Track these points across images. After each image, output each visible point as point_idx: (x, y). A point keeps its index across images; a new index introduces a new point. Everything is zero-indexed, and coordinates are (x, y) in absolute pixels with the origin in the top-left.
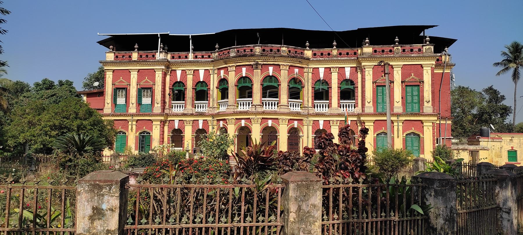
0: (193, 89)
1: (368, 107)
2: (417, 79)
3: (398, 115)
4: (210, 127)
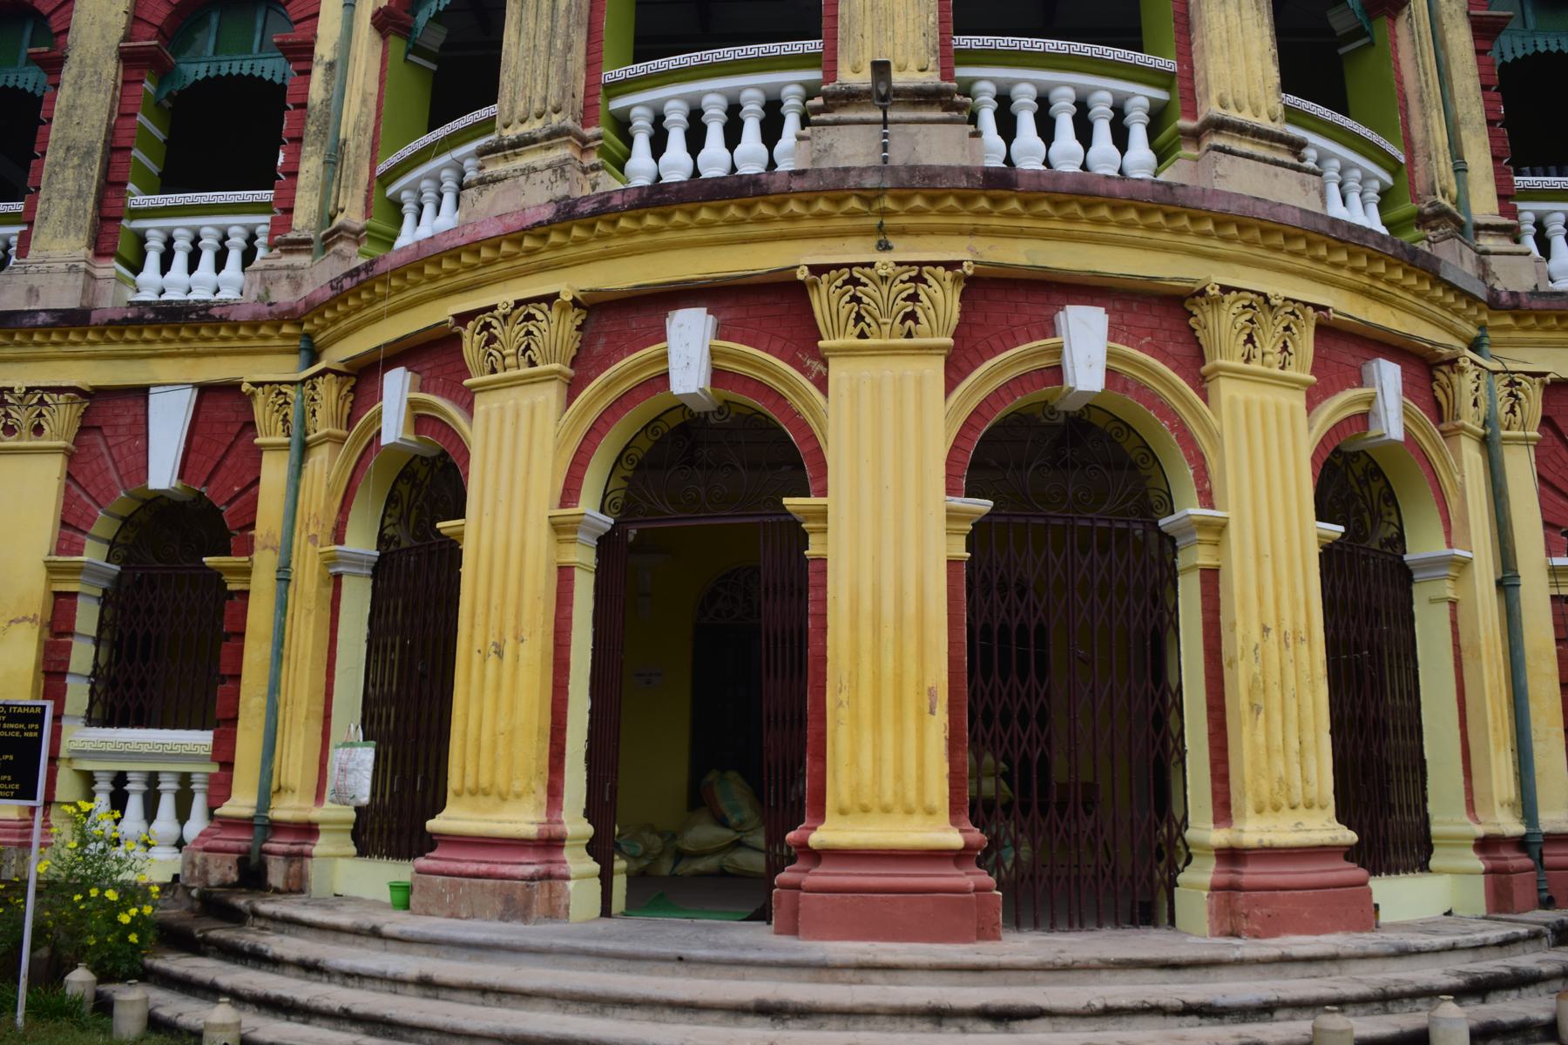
0: (128, 57)
4: (274, 472)
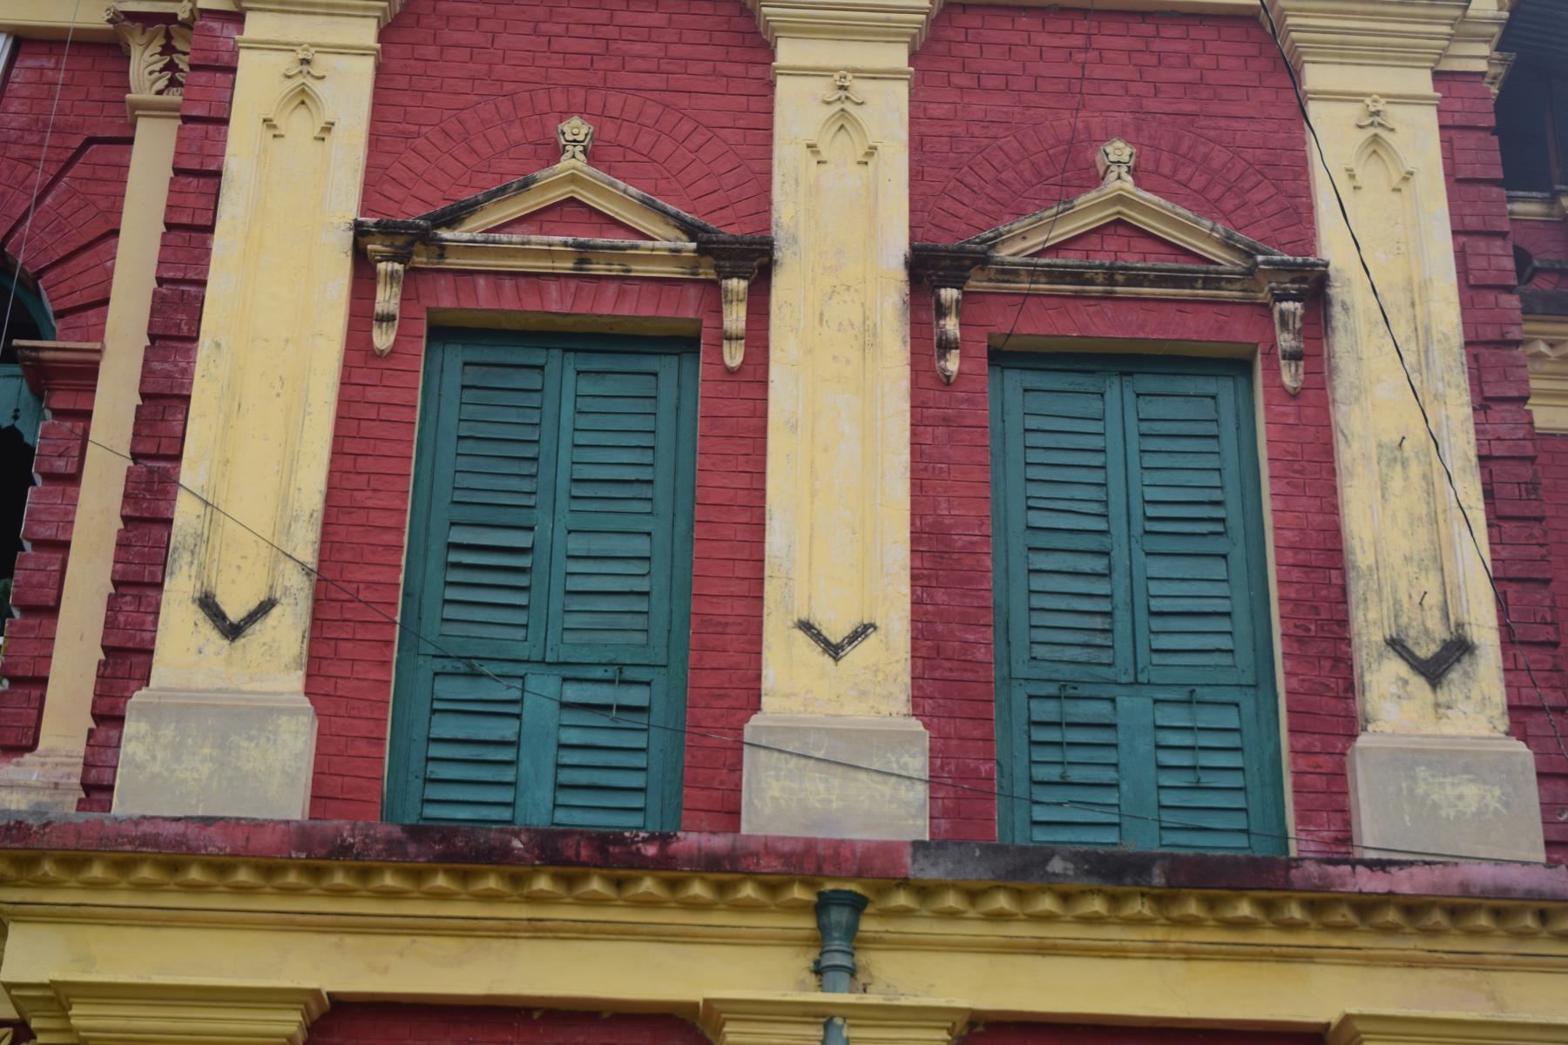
1: (187, 708)
2: (1202, 236)
3: (837, 894)
